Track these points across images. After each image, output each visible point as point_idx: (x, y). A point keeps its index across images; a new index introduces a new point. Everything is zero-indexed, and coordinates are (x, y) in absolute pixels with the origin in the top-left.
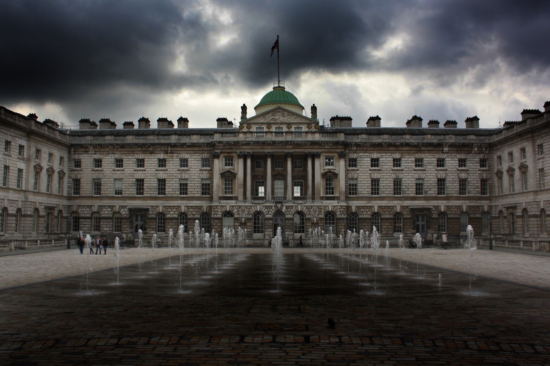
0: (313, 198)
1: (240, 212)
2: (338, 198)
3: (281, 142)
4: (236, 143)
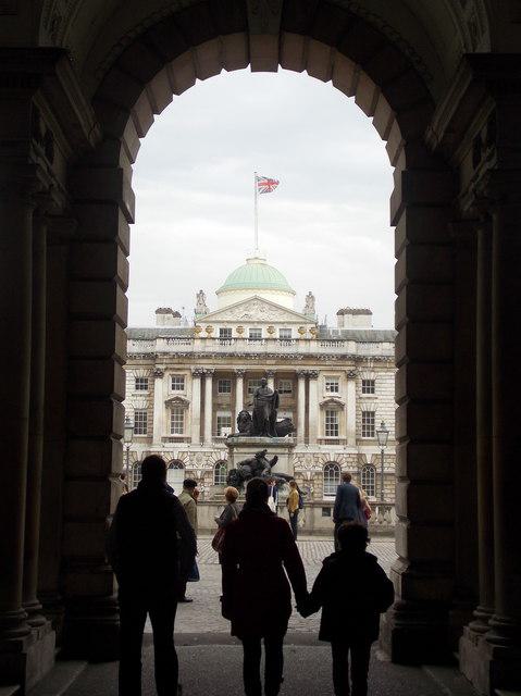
0: (307, 442)
1: (195, 462)
2: (345, 442)
3: (259, 355)
4: (190, 356)
